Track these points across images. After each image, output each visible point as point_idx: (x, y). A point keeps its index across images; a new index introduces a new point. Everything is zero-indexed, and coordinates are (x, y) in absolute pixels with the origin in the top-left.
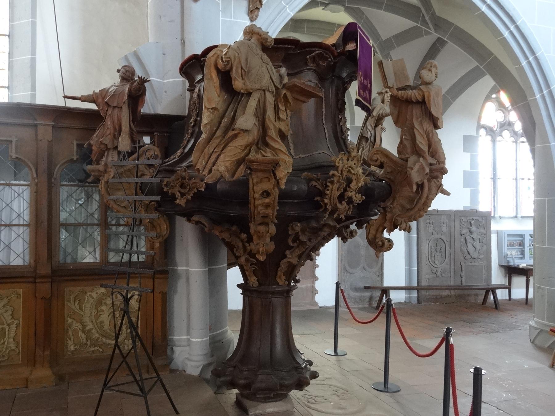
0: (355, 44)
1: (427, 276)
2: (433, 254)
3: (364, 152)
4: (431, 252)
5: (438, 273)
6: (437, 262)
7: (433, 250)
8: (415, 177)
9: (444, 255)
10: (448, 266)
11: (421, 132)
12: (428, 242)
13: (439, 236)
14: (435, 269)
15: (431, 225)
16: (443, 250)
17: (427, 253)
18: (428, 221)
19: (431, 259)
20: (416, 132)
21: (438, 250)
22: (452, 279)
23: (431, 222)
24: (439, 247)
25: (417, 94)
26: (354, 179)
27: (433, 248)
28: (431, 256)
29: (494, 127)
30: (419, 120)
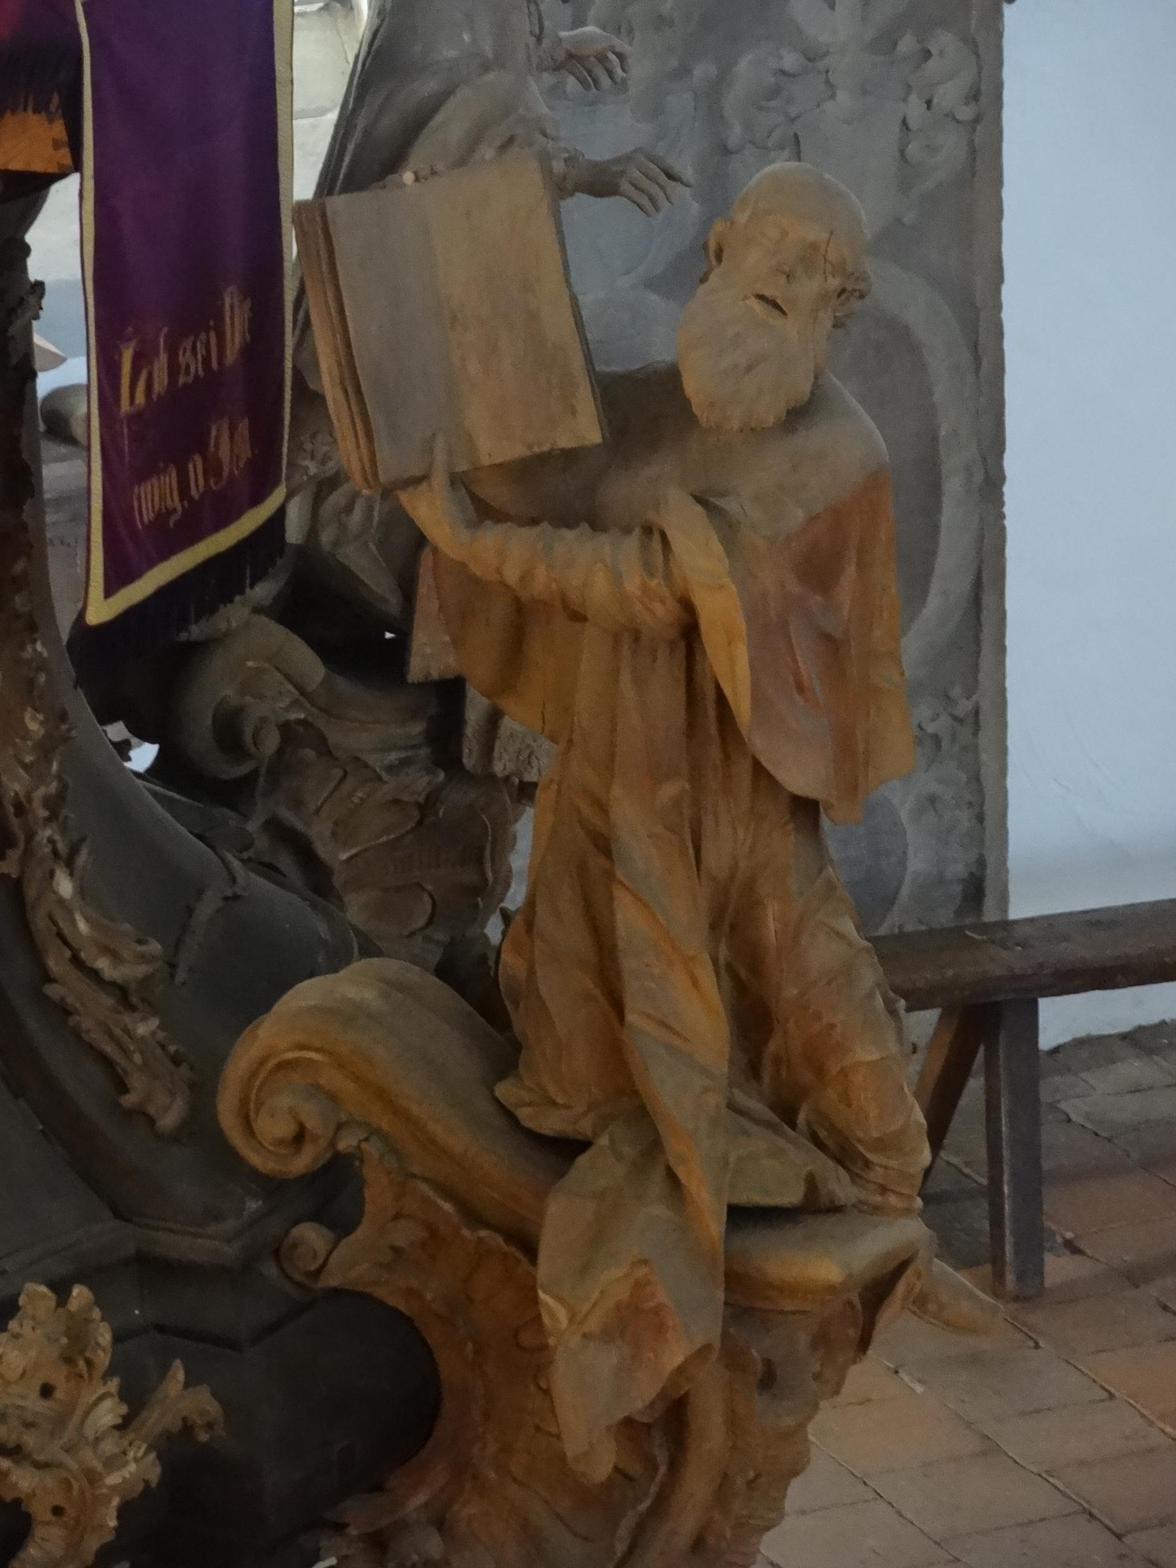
0: (59, 129)
3: (337, 498)
8: (589, 1396)
20: (628, 918)
25: (632, 586)
26: (40, 1511)
30: (669, 790)
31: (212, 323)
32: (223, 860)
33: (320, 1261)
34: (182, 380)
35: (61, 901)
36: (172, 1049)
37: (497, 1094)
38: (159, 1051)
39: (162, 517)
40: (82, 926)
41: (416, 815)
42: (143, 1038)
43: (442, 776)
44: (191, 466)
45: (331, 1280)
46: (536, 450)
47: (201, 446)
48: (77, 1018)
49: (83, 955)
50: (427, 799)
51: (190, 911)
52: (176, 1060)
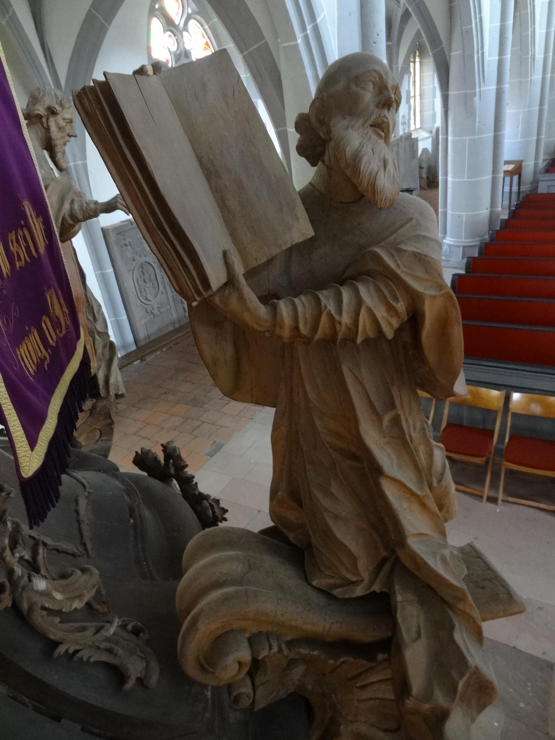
1: (144, 321)
2: (142, 288)
4: (138, 284)
5: (156, 311)
6: (149, 297)
7: (141, 282)
9: (155, 284)
10: (164, 296)
11: (408, 478)
12: (131, 273)
13: (143, 259)
14: (149, 309)
15: (129, 247)
16: (153, 277)
17: (134, 290)
18: (123, 242)
19: (141, 295)
20: (390, 492)
21: (147, 280)
22: (173, 311)
23: (127, 243)
24: (147, 276)
25: (381, 313)
27: (140, 279)
28: (141, 292)
29: (168, 61)
31: (23, 223)
32: (75, 478)
33: (252, 698)
34: (18, 264)
35: (42, 594)
36: (130, 627)
37: (314, 583)
38: (124, 634)
39: (40, 365)
40: (58, 596)
41: (89, 412)
42: (114, 634)
43: (95, 400)
44: (43, 325)
45: (260, 705)
46: (284, 248)
47: (44, 309)
48: (79, 655)
49: (64, 610)
50: (92, 407)
51: (77, 512)
52: (136, 632)
